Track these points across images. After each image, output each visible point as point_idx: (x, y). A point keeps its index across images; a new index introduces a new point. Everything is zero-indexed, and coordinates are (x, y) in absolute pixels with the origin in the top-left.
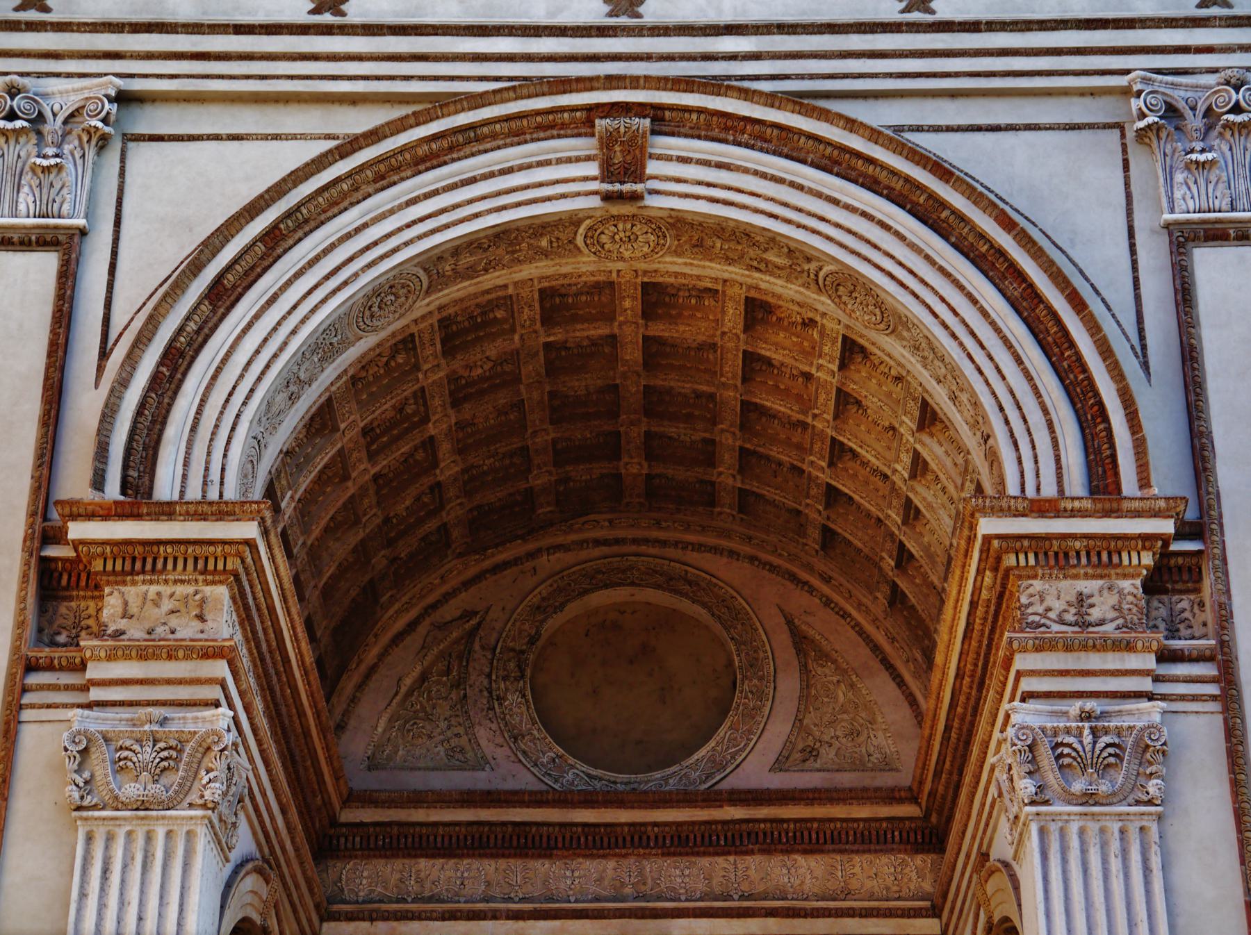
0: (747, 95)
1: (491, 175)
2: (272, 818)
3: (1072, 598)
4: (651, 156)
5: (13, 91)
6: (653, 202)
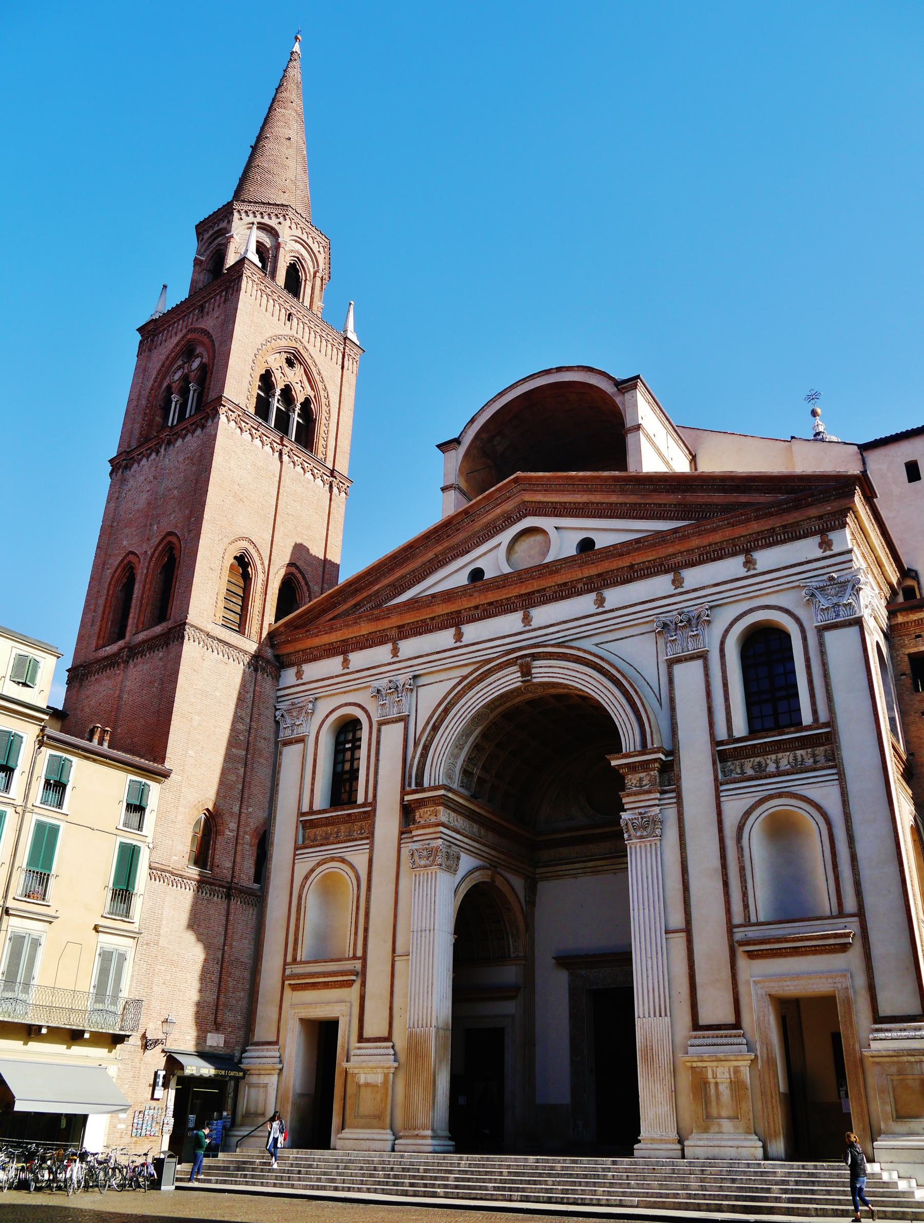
0: (552, 646)
1: (495, 681)
3: (638, 779)
4: (533, 668)
5: (390, 681)
6: (535, 680)
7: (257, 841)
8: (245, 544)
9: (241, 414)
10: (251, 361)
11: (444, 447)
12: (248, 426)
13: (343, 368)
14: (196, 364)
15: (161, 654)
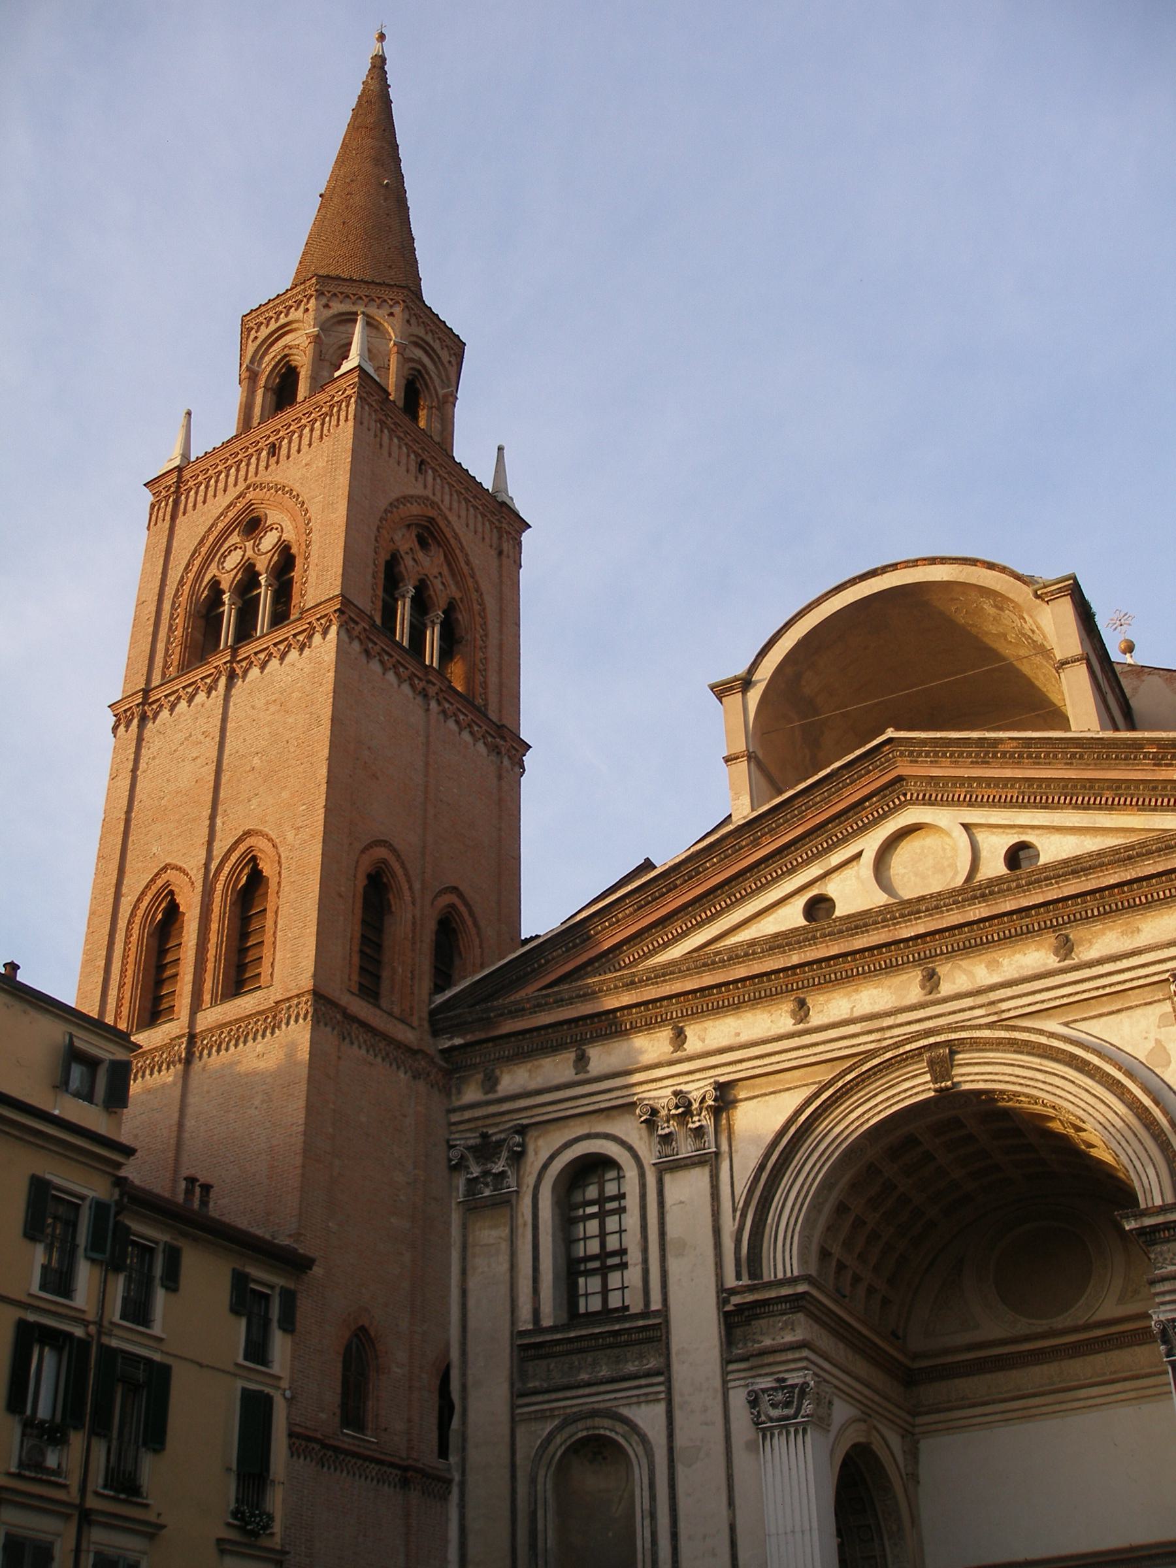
0: (990, 1026)
2: (861, 1394)
8: (382, 852)
9: (367, 627)
10: (373, 539)
11: (721, 690)
12: (377, 649)
13: (500, 553)
14: (269, 541)
15: (259, 1048)
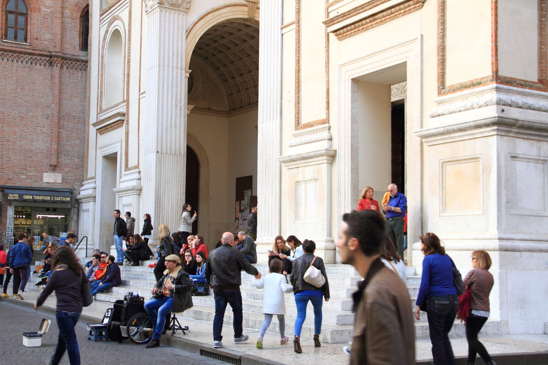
7: (79, 15)
